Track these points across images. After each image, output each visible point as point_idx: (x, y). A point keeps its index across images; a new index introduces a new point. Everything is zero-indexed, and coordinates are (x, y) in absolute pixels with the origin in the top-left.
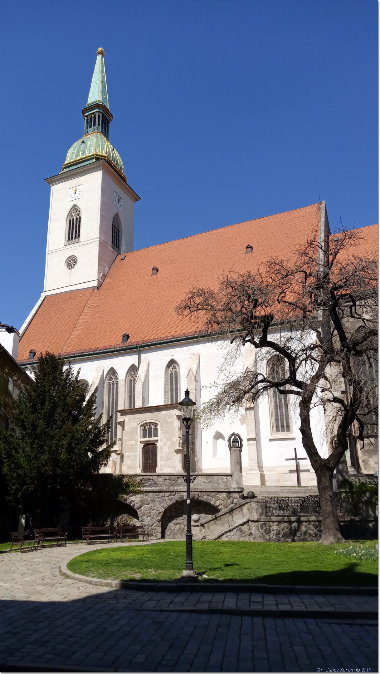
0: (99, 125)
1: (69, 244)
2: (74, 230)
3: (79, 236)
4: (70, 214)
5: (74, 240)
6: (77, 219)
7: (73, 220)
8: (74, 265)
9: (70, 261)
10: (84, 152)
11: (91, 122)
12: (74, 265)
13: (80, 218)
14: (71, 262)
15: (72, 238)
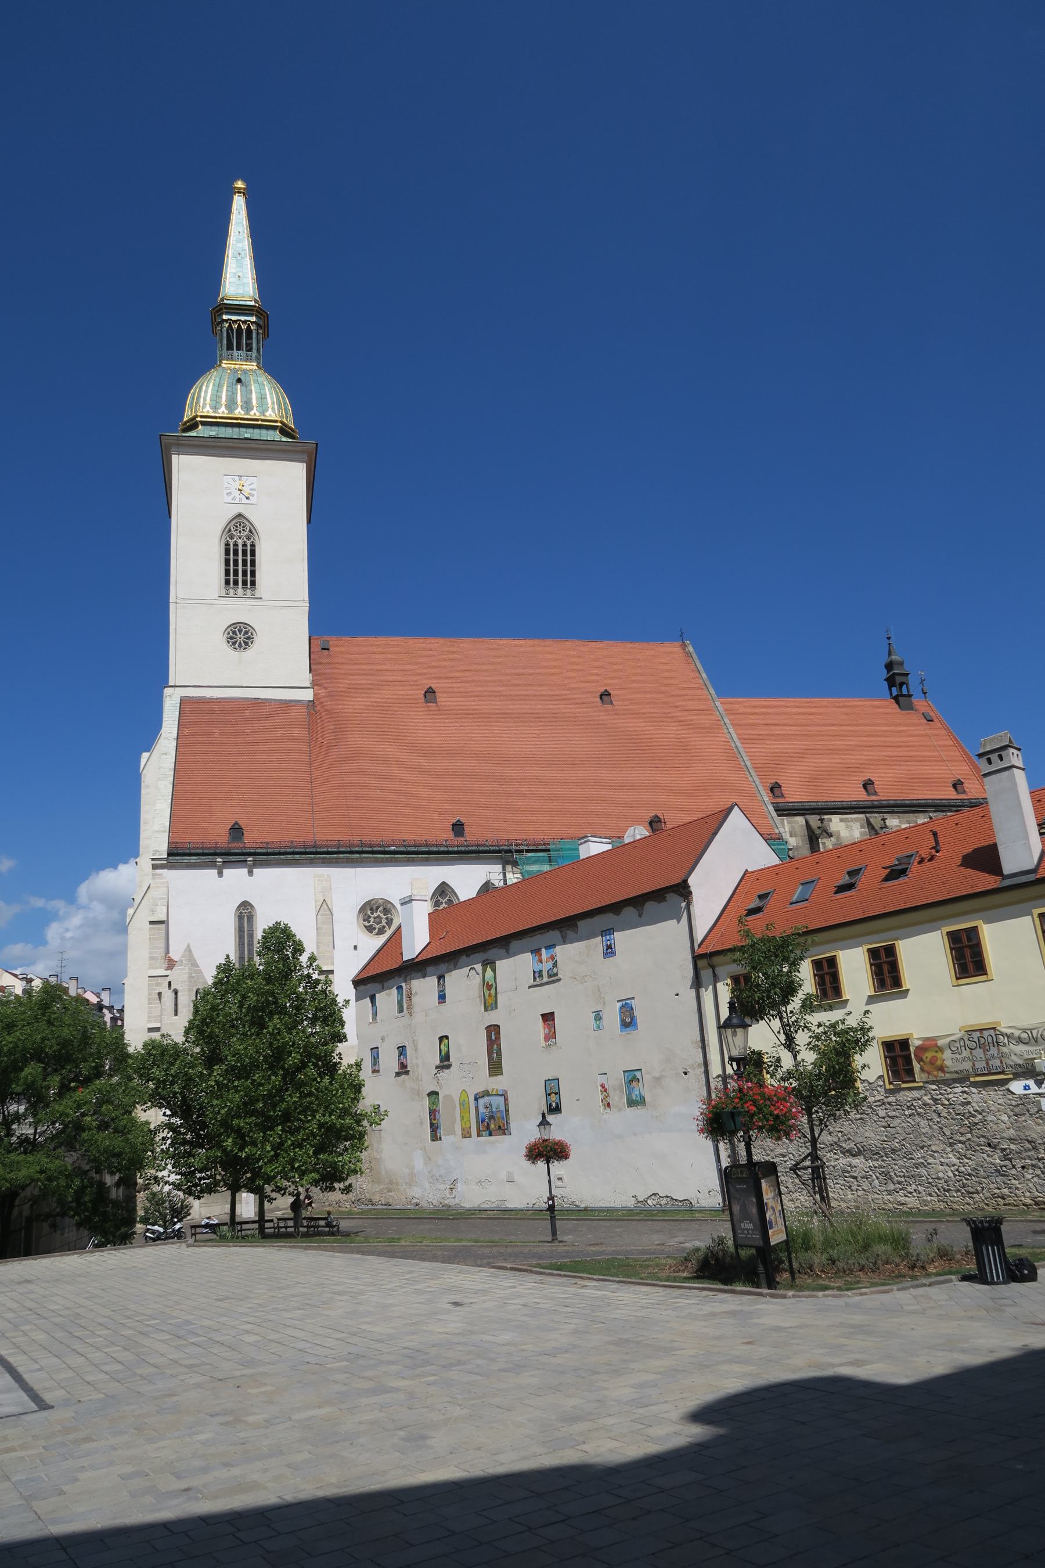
0: (258, 350)
1: (227, 596)
2: (240, 566)
3: (253, 583)
4: (228, 531)
5: (240, 591)
6: (245, 545)
7: (236, 545)
8: (246, 644)
9: (234, 633)
10: (247, 406)
11: (239, 341)
12: (246, 644)
13: (253, 545)
14: (240, 636)
15: (236, 583)
